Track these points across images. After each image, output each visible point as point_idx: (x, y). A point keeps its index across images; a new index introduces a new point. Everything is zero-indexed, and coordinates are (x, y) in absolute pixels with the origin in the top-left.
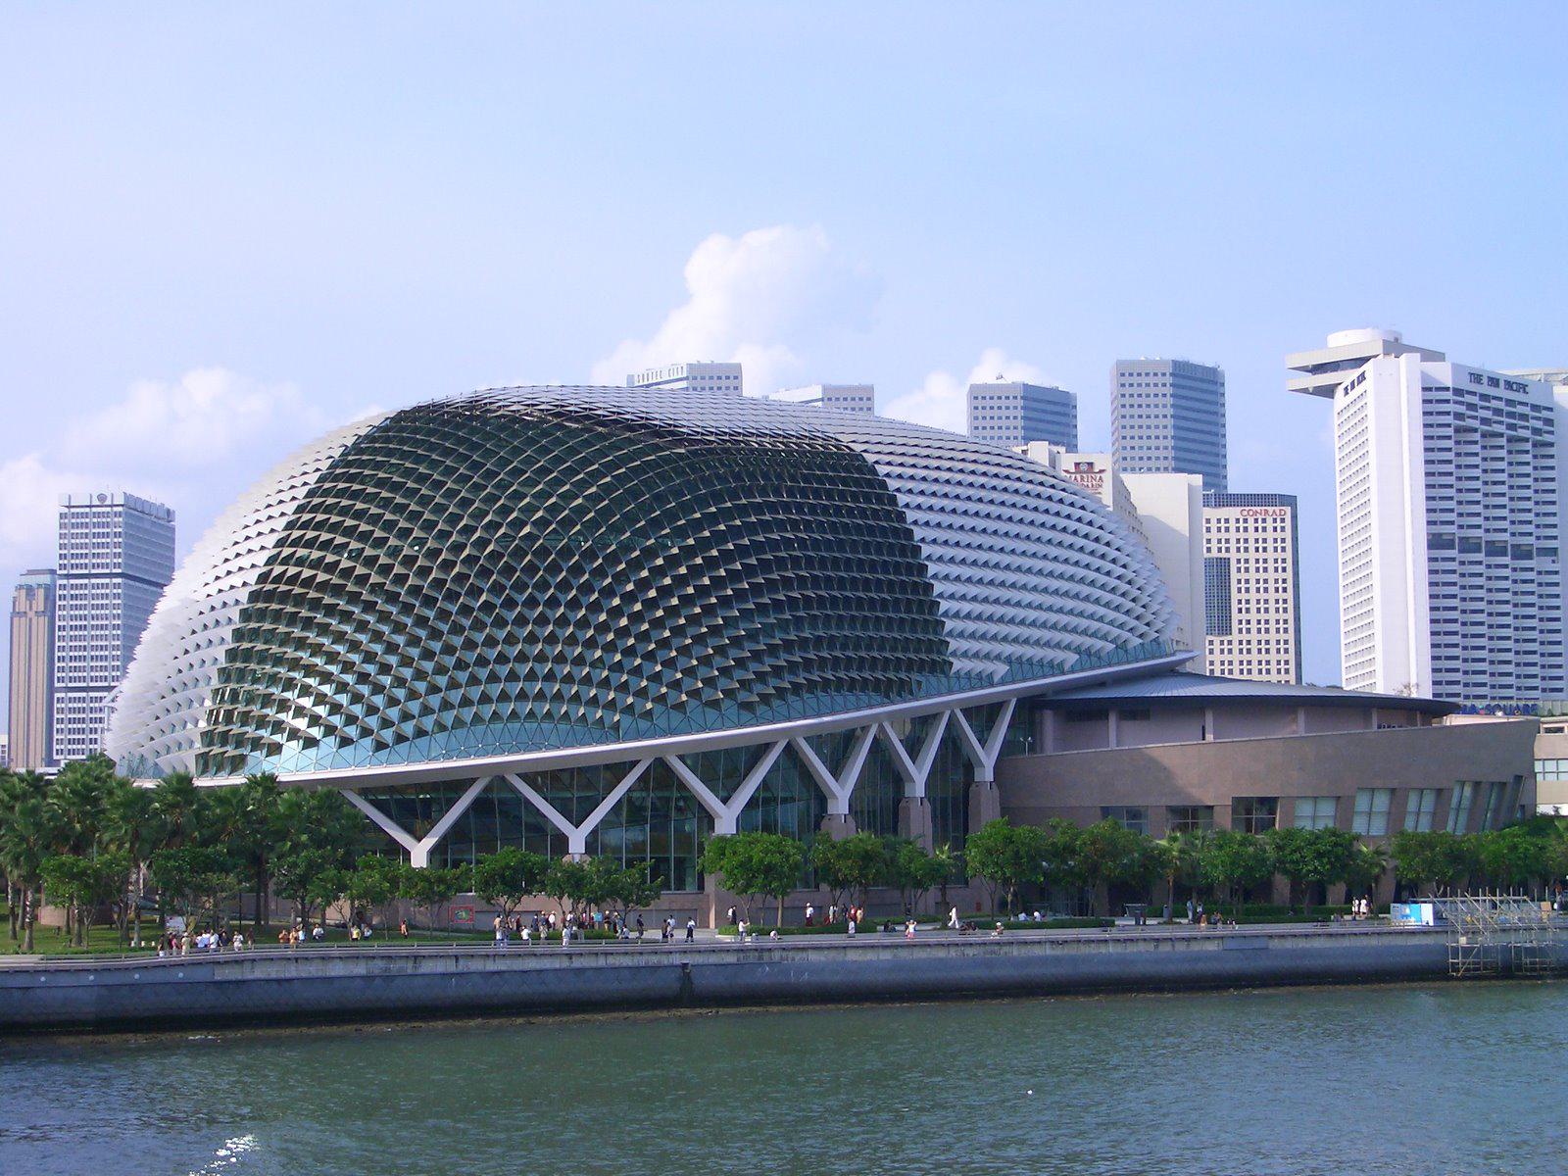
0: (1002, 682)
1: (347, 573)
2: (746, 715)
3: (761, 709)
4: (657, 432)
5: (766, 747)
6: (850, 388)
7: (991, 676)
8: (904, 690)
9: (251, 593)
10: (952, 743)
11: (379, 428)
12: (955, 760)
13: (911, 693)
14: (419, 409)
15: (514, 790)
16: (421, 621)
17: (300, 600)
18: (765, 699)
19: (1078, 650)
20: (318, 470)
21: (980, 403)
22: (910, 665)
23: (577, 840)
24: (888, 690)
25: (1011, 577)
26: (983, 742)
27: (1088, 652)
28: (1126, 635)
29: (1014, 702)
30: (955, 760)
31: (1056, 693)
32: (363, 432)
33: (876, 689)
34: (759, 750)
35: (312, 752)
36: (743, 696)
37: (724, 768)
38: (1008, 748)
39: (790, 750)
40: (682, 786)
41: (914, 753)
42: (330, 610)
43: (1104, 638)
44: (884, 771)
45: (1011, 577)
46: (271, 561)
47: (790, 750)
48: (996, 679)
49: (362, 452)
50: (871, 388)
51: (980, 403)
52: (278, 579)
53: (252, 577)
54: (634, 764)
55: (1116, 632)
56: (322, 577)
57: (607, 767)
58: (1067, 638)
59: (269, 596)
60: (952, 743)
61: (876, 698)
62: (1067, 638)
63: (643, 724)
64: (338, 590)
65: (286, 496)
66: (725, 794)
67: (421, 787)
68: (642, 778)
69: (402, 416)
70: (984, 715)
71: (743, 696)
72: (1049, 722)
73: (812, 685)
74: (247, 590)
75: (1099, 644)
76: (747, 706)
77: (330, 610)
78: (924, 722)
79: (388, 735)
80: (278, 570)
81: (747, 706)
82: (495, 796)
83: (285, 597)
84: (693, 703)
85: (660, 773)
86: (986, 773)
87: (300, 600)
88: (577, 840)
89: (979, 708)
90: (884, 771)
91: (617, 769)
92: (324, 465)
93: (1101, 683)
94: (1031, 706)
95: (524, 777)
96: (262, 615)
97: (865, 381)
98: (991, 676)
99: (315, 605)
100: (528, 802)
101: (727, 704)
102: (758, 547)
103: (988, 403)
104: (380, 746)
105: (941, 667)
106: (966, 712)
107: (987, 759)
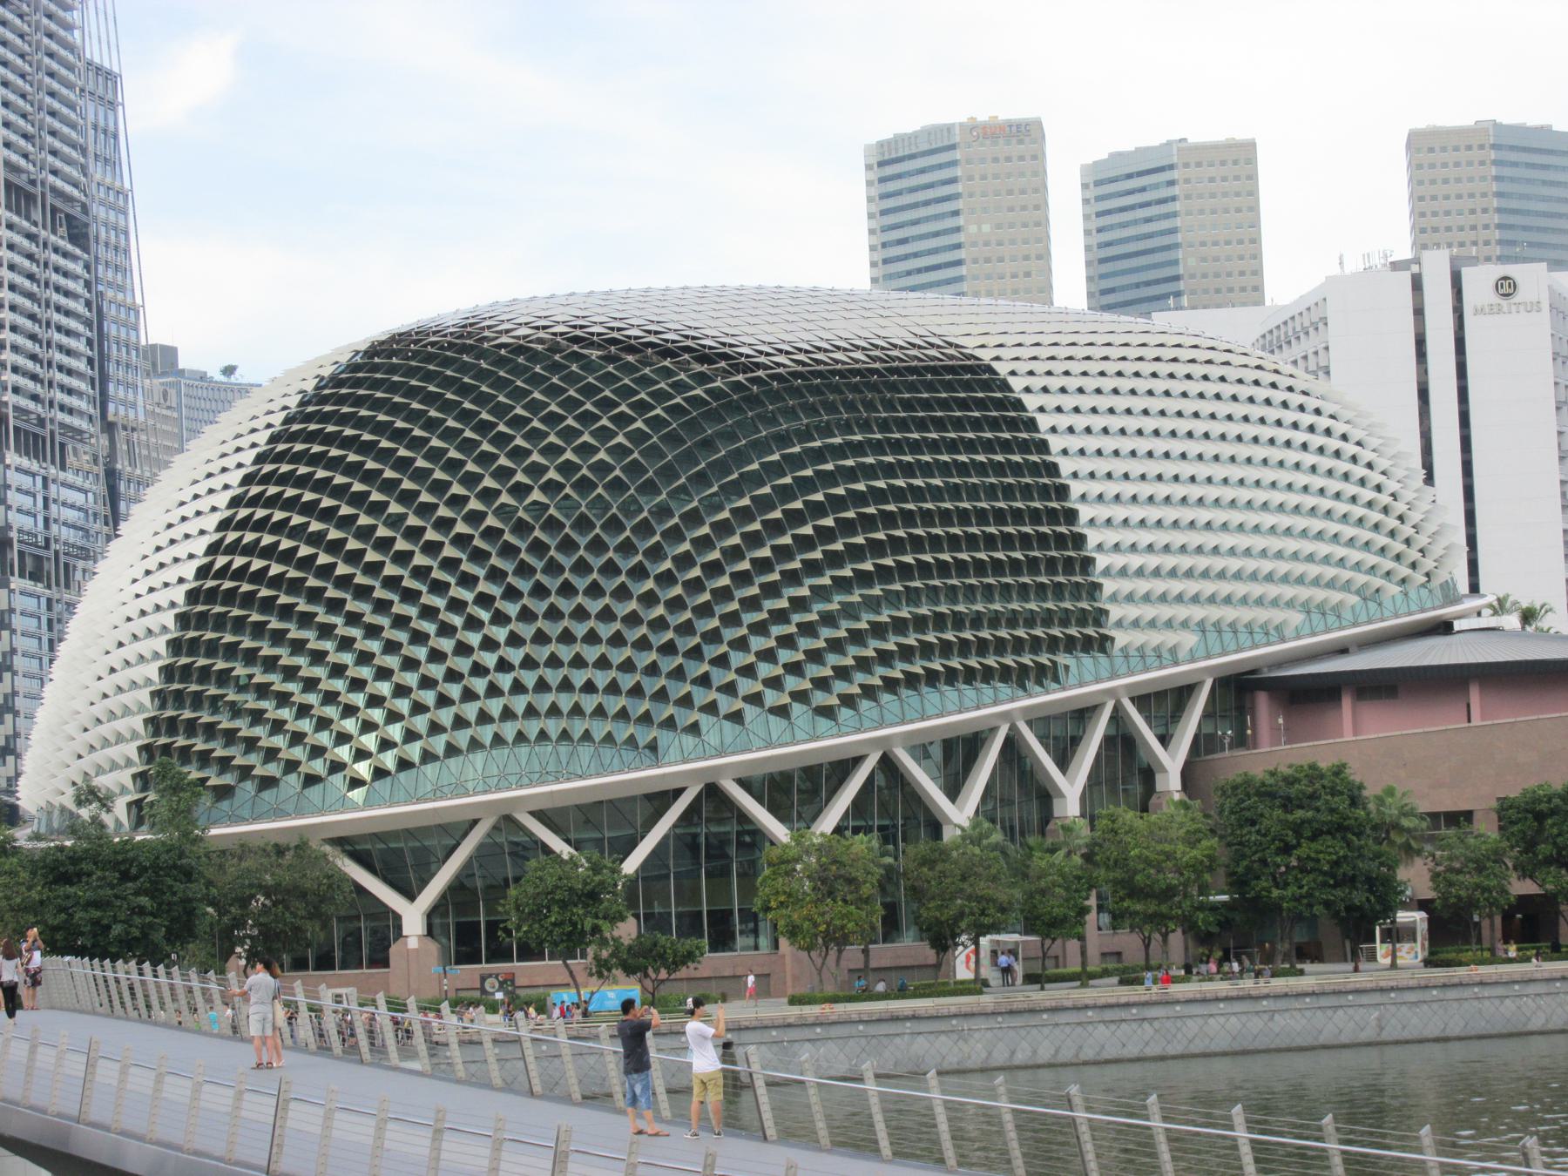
2: (823, 723)
3: (845, 713)
4: (705, 357)
6: (1215, 147)
7: (1173, 650)
8: (1044, 675)
10: (1121, 742)
12: (1125, 764)
13: (1056, 679)
17: (248, 600)
18: (848, 701)
22: (1053, 644)
24: (1020, 677)
26: (1164, 740)
27: (1322, 609)
28: (1378, 582)
30: (1125, 764)
31: (1272, 667)
32: (327, 372)
34: (843, 768)
35: (267, 795)
36: (820, 698)
37: (797, 790)
38: (1202, 745)
39: (888, 764)
40: (743, 817)
41: (1063, 763)
42: (286, 612)
43: (1347, 586)
44: (1021, 787)
47: (888, 764)
48: (1181, 655)
49: (324, 400)
53: (189, 570)
54: (678, 792)
55: (1361, 579)
57: (649, 797)
58: (1182, 612)
59: (212, 596)
60: (1121, 742)
61: (1004, 689)
62: (1288, 592)
63: (689, 741)
64: (295, 586)
67: (410, 833)
69: (376, 350)
70: (1165, 703)
71: (820, 698)
75: (1336, 597)
76: (826, 712)
77: (286, 612)
78: (1083, 714)
79: (363, 769)
80: (221, 561)
82: (501, 839)
86: (1171, 781)
89: (1160, 695)
90: (1021, 787)
91: (661, 799)
93: (1342, 650)
95: (539, 815)
96: (202, 620)
97: (1241, 135)
98: (1173, 650)
99: (267, 605)
101: (797, 709)
102: (837, 503)
104: (356, 783)
106: (1142, 701)
107: (1171, 762)
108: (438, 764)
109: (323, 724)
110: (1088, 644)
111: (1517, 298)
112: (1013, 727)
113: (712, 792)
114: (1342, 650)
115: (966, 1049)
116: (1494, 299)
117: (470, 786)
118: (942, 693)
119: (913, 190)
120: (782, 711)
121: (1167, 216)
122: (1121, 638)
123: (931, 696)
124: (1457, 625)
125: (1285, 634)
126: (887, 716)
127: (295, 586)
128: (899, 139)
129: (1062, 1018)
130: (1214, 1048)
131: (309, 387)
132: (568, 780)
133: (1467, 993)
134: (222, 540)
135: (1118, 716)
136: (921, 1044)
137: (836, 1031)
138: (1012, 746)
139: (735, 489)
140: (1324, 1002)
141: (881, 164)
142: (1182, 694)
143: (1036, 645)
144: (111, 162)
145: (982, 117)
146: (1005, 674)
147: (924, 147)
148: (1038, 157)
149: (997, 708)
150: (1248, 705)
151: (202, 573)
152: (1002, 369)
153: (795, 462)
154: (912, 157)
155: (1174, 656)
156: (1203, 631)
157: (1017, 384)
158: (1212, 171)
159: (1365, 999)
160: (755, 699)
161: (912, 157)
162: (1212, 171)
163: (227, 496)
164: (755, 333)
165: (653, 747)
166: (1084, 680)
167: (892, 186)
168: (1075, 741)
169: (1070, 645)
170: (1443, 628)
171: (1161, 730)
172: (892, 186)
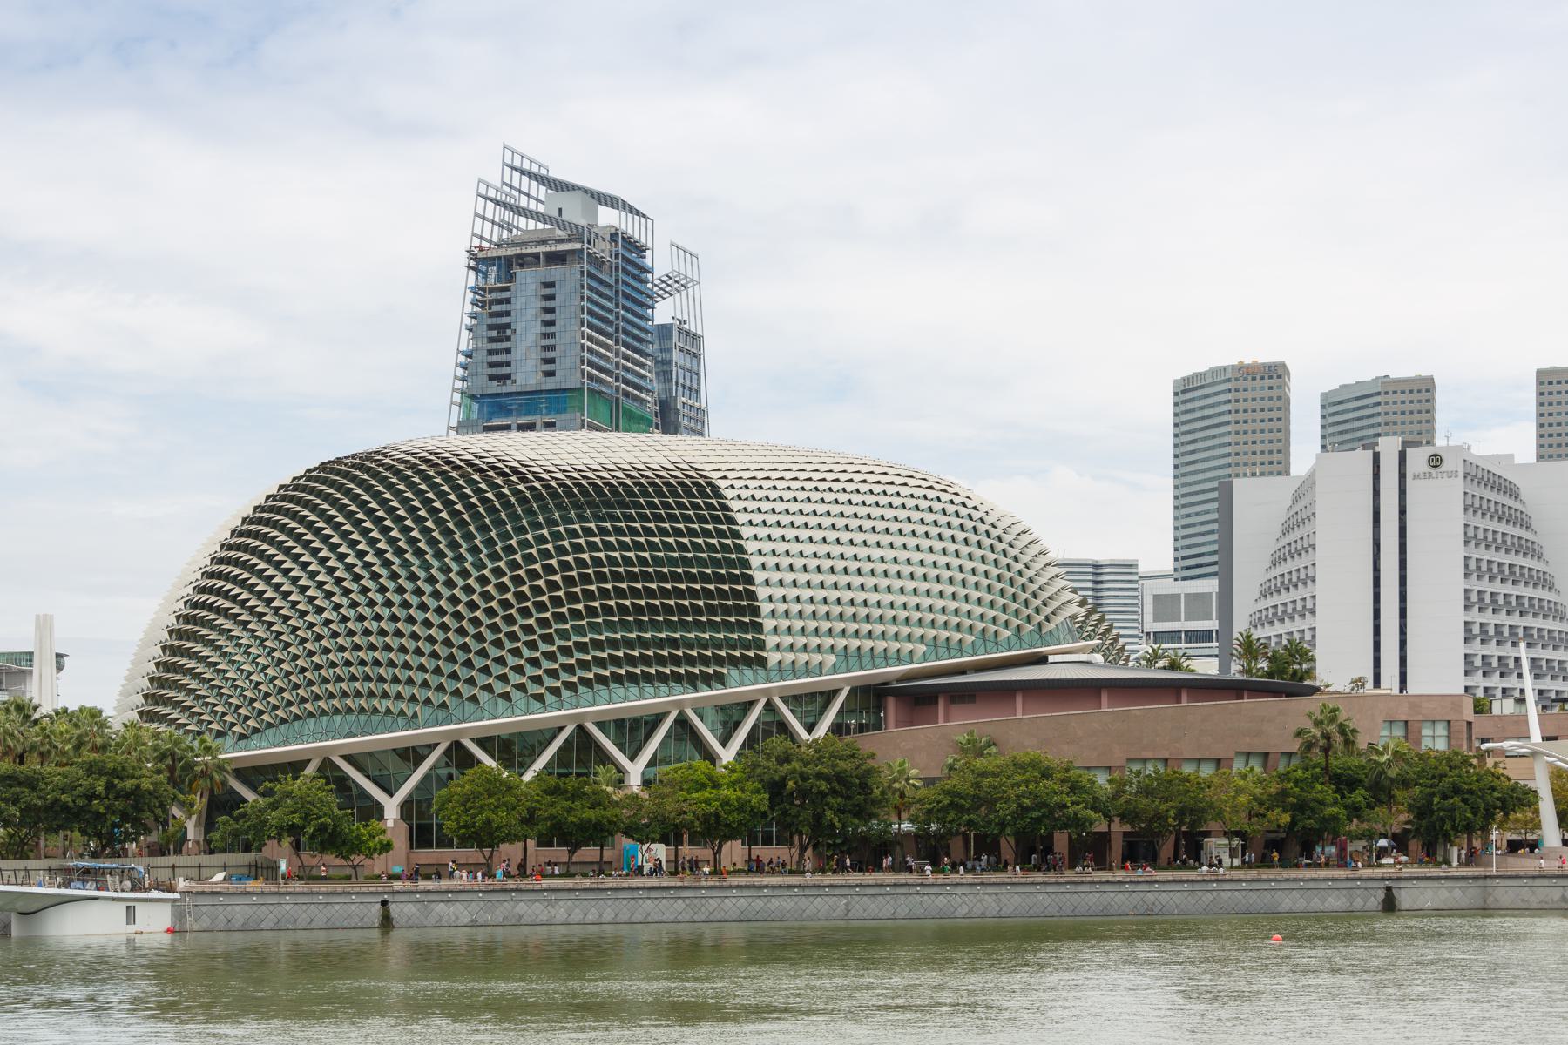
0: (835, 669)
2: (537, 705)
3: (550, 698)
5: (561, 729)
8: (707, 680)
18: (555, 692)
21: (1546, 388)
22: (719, 661)
23: (392, 807)
24: (692, 681)
31: (899, 680)
39: (581, 728)
50: (1431, 380)
51: (1546, 388)
54: (432, 747)
63: (442, 714)
64: (225, 613)
69: (323, 467)
70: (813, 702)
72: (891, 703)
73: (633, 678)
76: (540, 698)
81: (540, 698)
85: (458, 755)
88: (392, 807)
93: (961, 670)
95: (348, 758)
97: (1425, 373)
103: (1555, 388)
104: (242, 737)
106: (785, 700)
110: (747, 661)
111: (1444, 468)
112: (681, 713)
114: (963, 673)
115: (553, 911)
116: (1427, 469)
119: (1202, 408)
120: (506, 696)
121: (1372, 426)
122: (773, 658)
123: (618, 690)
124: (1051, 659)
125: (909, 657)
127: (225, 613)
128: (1196, 376)
129: (622, 895)
130: (727, 917)
133: (912, 891)
135: (769, 706)
136: (521, 908)
137: (462, 897)
138: (682, 723)
140: (807, 892)
141: (1184, 392)
142: (829, 696)
143: (705, 660)
144: (694, 392)
145: (1247, 361)
146: (678, 678)
147: (1209, 381)
148: (1283, 386)
152: (722, 484)
154: (1202, 387)
156: (846, 656)
157: (729, 493)
158: (1403, 397)
159: (837, 891)
161: (1202, 387)
162: (1403, 397)
165: (415, 715)
166: (740, 685)
167: (1189, 406)
168: (737, 724)
169: (733, 662)
170: (1041, 660)
171: (810, 720)
172: (1189, 406)
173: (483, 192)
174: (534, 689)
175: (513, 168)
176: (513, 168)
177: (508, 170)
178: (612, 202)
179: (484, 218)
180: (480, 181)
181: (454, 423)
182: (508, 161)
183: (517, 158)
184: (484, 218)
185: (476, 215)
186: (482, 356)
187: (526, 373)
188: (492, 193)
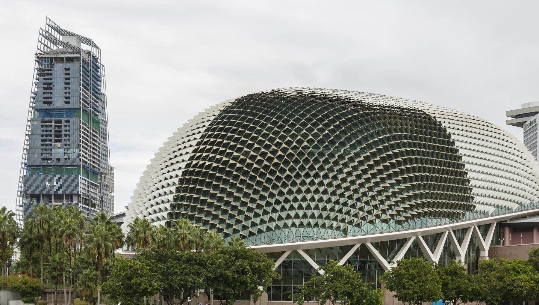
1: (225, 163)
9: (183, 172)
11: (224, 111)
14: (249, 95)
15: (300, 256)
16: (269, 181)
17: (205, 175)
19: (494, 206)
20: (209, 121)
25: (494, 171)
27: (521, 204)
29: (496, 223)
31: (510, 220)
33: (448, 217)
34: (402, 242)
40: (372, 256)
42: (218, 179)
45: (494, 171)
46: (192, 158)
48: (490, 214)
52: (195, 166)
54: (352, 246)
56: (215, 165)
59: (191, 173)
61: (448, 220)
62: (514, 198)
64: (222, 170)
65: (196, 131)
66: (389, 260)
68: (356, 253)
70: (485, 228)
74: (181, 171)
76: (399, 222)
77: (218, 179)
78: (464, 231)
80: (195, 162)
83: (198, 173)
84: (363, 222)
87: (205, 175)
91: (345, 249)
92: (212, 119)
93: (524, 217)
94: (502, 225)
95: (307, 251)
96: (188, 181)
99: (212, 176)
100: (307, 262)
105: (470, 208)
108: (255, 236)
109: (241, 213)
113: (364, 248)
117: (283, 239)
118: (426, 219)
122: (478, 207)
126: (411, 226)
127: (222, 170)
131: (217, 113)
132: (317, 240)
134: (195, 155)
135: (475, 231)
139: (370, 146)
144: (103, 115)
149: (444, 225)
150: (502, 231)
151: (188, 166)
153: (382, 141)
155: (509, 210)
160: (364, 218)
163: (196, 142)
164: (367, 100)
173: (41, 32)
174: (369, 218)
175: (49, 25)
176: (49, 25)
177: (47, 26)
178: (88, 42)
179: (41, 42)
180: (41, 29)
181: (29, 119)
182: (48, 23)
183: (51, 22)
184: (41, 42)
185: (39, 41)
186: (41, 95)
187: (58, 102)
188: (44, 33)
